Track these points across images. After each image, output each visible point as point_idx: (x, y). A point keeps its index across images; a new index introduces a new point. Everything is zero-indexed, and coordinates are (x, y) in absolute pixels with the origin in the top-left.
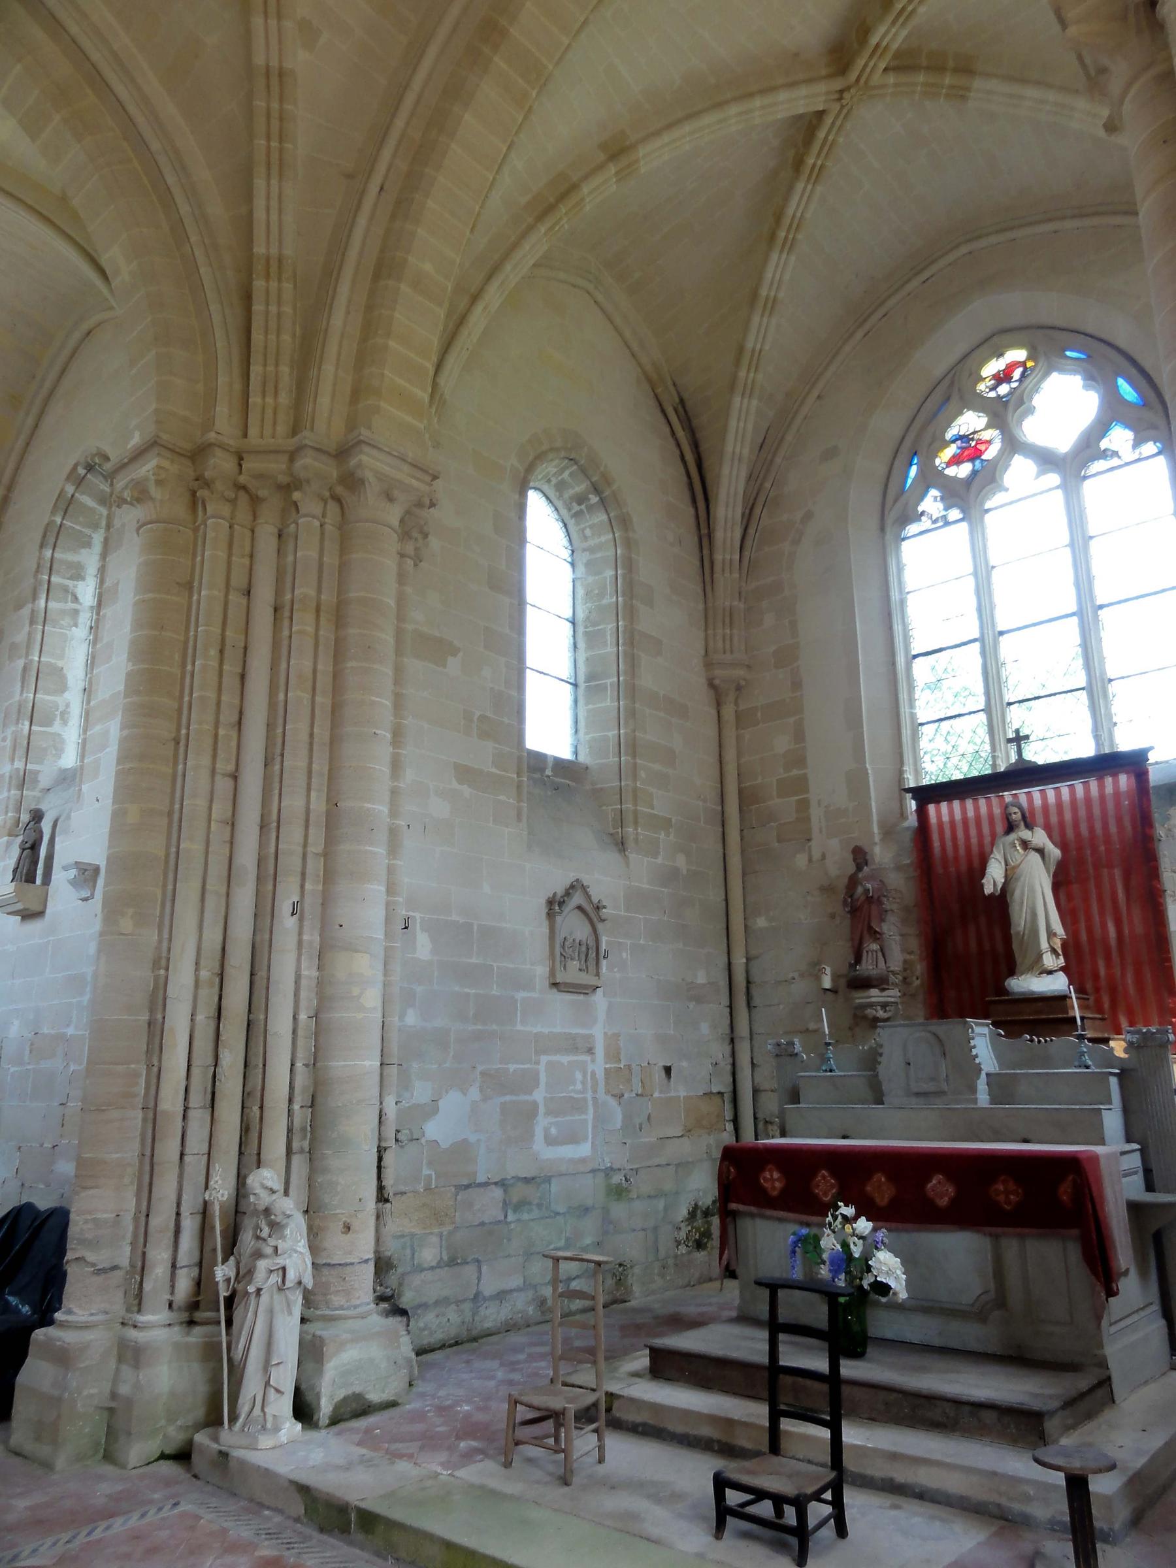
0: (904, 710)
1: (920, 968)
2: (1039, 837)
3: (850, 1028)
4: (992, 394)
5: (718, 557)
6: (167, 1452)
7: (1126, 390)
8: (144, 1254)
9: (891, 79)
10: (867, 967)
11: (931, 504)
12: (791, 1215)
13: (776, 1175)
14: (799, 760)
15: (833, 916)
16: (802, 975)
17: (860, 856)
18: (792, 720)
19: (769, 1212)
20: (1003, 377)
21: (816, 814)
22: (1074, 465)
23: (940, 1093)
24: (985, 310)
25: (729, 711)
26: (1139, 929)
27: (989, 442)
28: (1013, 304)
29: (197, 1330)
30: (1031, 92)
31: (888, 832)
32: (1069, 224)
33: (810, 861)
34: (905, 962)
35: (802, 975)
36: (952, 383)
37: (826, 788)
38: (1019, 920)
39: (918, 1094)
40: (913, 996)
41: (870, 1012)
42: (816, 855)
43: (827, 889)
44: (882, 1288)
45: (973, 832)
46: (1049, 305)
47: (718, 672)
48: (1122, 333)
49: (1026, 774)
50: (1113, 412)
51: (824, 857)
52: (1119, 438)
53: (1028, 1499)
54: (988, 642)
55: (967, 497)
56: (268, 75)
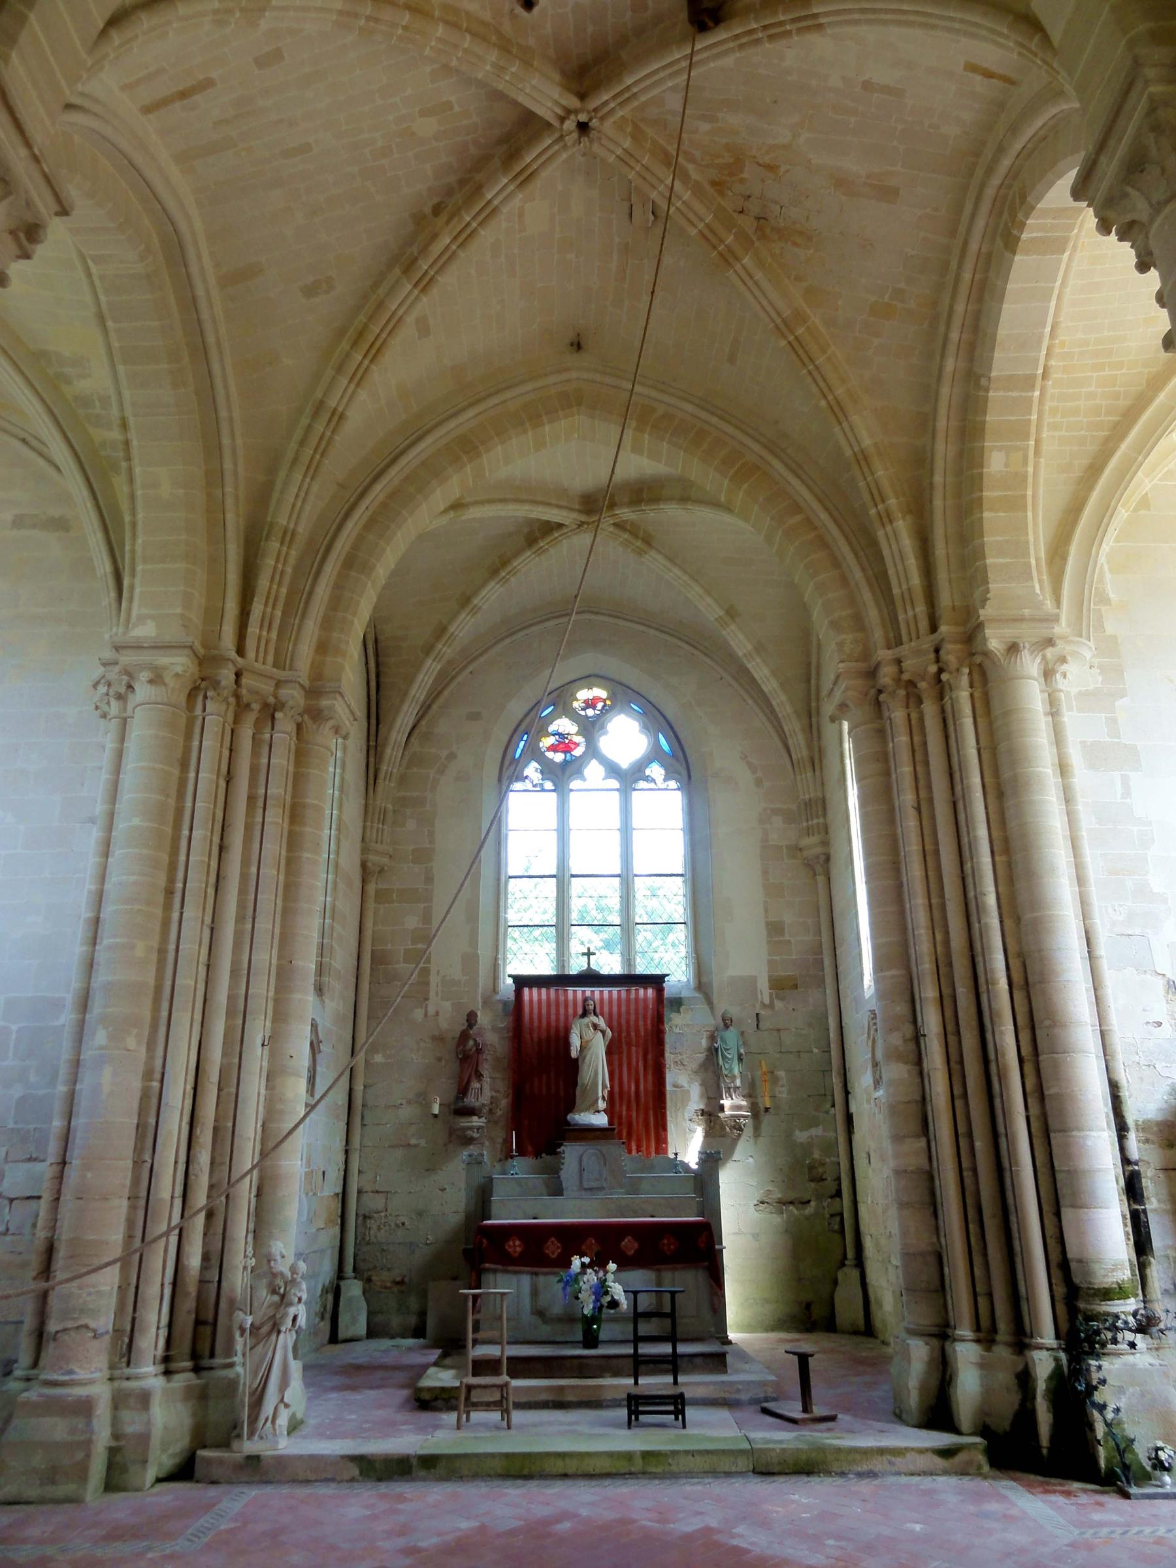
0: (502, 914)
1: (504, 1103)
2: (601, 1022)
3: (445, 1145)
4: (583, 713)
5: (384, 768)
6: (160, 1476)
7: (665, 746)
8: (134, 1319)
9: (611, 529)
10: (471, 1100)
12: (522, 1268)
13: (517, 1243)
15: (440, 1059)
16: (409, 1102)
17: (471, 1018)
18: (422, 905)
19: (510, 1268)
20: (590, 704)
21: (434, 980)
22: (629, 779)
23: (601, 1189)
25: (371, 888)
26: (650, 1087)
27: (577, 745)
28: (611, 664)
29: (177, 1377)
30: (676, 570)
31: (487, 1002)
32: (652, 632)
33: (426, 1015)
34: (492, 1097)
35: (409, 1102)
36: (559, 696)
37: (445, 960)
39: (586, 1189)
40: (496, 1123)
41: (469, 1133)
42: (431, 1010)
43: (439, 1039)
44: (614, 1304)
45: (553, 1011)
46: (631, 675)
47: (371, 857)
48: (671, 710)
49: (590, 978)
50: (656, 754)
51: (437, 1014)
52: (656, 771)
53: (738, 1391)
54: (563, 878)
56: (333, 414)
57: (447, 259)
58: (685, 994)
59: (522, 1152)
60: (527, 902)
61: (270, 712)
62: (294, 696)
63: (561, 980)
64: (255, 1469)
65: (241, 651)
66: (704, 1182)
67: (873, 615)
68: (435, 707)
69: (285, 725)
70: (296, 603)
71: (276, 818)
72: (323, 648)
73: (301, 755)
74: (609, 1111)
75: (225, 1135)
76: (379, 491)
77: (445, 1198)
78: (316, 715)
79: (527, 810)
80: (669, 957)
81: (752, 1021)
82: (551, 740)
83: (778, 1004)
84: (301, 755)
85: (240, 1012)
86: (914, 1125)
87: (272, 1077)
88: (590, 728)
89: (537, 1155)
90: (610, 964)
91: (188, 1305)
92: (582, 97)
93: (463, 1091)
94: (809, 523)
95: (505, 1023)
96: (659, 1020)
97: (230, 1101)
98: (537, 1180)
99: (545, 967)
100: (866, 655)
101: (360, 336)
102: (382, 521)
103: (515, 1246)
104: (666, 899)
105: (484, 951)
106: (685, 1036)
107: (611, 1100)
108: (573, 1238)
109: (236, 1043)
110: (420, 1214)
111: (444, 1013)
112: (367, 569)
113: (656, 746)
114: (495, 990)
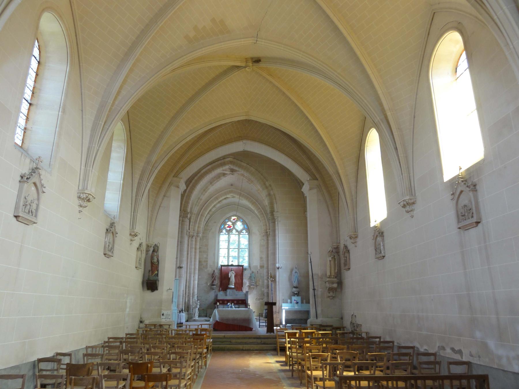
1: (219, 284)
10: (214, 283)
11: (224, 231)
14: (207, 258)
17: (214, 271)
20: (234, 220)
21: (208, 265)
22: (239, 232)
24: (234, 213)
31: (216, 268)
37: (210, 262)
38: (231, 280)
43: (209, 274)
49: (232, 265)
52: (244, 231)
60: (223, 252)
61: (193, 237)
62: (195, 234)
63: (228, 266)
64: (195, 321)
66: (246, 294)
67: (268, 225)
71: (193, 250)
72: (198, 227)
73: (196, 241)
74: (235, 285)
75: (189, 287)
77: (211, 297)
78: (198, 236)
79: (223, 237)
82: (227, 226)
84: (196, 241)
85: (190, 273)
87: (194, 281)
88: (234, 224)
90: (235, 263)
93: (213, 282)
95: (219, 272)
96: (243, 272)
100: (267, 230)
102: (206, 209)
106: (246, 274)
107: (235, 283)
108: (228, 301)
109: (190, 277)
111: (210, 270)
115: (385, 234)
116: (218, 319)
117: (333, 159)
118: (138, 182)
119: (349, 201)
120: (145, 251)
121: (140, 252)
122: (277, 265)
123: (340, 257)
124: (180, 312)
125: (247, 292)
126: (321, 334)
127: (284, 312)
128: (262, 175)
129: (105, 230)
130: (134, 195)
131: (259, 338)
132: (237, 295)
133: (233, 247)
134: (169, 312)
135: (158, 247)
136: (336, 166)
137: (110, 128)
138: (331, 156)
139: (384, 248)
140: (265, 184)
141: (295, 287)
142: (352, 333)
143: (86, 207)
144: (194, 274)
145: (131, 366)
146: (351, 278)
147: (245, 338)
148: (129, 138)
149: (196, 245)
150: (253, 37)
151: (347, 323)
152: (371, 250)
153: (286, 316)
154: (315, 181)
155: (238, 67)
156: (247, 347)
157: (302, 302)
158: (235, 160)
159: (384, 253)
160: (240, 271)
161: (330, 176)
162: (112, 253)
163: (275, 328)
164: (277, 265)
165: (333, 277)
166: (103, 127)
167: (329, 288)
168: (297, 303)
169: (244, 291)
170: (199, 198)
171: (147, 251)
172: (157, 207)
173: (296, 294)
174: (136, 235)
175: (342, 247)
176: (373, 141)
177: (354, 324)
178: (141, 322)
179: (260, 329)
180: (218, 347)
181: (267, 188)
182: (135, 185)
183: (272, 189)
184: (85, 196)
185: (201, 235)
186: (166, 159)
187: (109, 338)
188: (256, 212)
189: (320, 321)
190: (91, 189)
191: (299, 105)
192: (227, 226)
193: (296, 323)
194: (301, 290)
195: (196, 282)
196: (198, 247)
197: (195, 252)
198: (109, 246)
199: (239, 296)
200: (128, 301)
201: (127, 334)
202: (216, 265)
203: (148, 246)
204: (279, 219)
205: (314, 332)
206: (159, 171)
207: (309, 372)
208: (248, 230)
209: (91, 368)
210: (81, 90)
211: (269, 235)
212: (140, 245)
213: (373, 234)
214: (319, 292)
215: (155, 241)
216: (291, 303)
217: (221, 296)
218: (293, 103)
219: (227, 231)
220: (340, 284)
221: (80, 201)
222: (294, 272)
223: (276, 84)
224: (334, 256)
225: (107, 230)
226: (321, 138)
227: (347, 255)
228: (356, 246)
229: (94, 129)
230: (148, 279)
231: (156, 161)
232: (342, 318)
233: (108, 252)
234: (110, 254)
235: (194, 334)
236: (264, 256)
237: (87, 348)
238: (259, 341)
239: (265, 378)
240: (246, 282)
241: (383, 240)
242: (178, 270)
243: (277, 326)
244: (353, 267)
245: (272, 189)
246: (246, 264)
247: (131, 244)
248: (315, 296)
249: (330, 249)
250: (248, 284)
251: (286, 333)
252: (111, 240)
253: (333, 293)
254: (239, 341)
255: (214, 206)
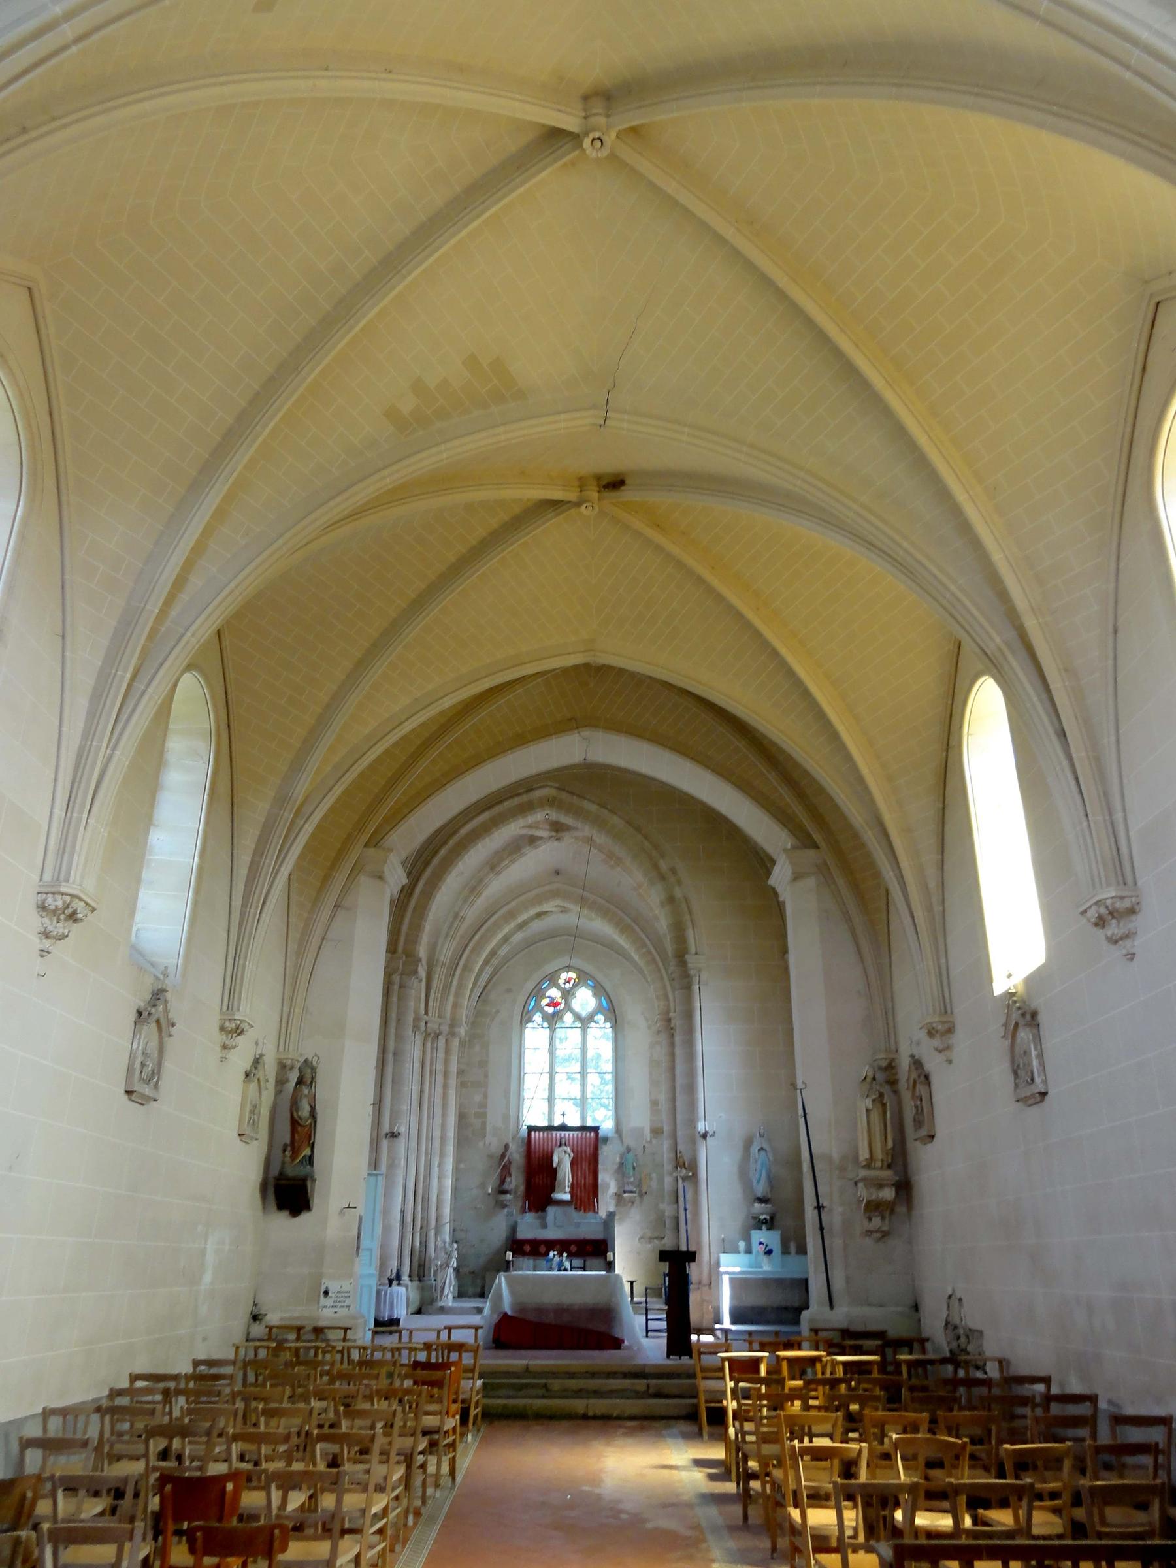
1: (522, 1189)
2: (569, 1150)
11: (537, 1017)
14: (483, 1105)
17: (506, 1147)
21: (489, 1128)
22: (585, 1022)
28: (577, 962)
37: (494, 1119)
38: (560, 1175)
43: (491, 1156)
49: (563, 1127)
52: (600, 1018)
55: (553, 1020)
57: (507, 866)
58: (610, 1135)
59: (530, 1210)
62: (445, 1029)
63: (550, 1128)
65: (426, 1013)
68: (489, 987)
69: (442, 1040)
70: (446, 990)
71: (439, 1078)
72: (455, 1005)
73: (447, 1051)
74: (572, 1193)
75: (426, 1200)
76: (477, 937)
77: (496, 1230)
78: (452, 1034)
79: (535, 1036)
80: (604, 1119)
81: (640, 1149)
82: (547, 1001)
83: (654, 1141)
84: (447, 1051)
85: (429, 1155)
86: (673, 1198)
88: (567, 994)
89: (537, 1211)
90: (574, 1121)
91: (416, 1259)
92: (557, 831)
93: (503, 1182)
94: (650, 952)
95: (523, 1149)
96: (596, 1148)
97: (427, 1188)
98: (537, 1222)
99: (544, 1123)
101: (474, 888)
103: (527, 1248)
104: (601, 1087)
105: (512, 1113)
106: (609, 1157)
108: (551, 1245)
109: (428, 1166)
110: (482, 1241)
111: (493, 1144)
112: (471, 970)
113: (600, 1004)
114: (518, 1131)
115: (1042, 1018)
116: (507, 1307)
117: (861, 779)
118: (252, 862)
119: (919, 914)
120: (272, 1081)
121: (253, 1086)
122: (701, 1127)
123: (898, 1098)
124: (391, 1282)
125: (611, 1215)
126: (845, 1364)
127: (726, 1280)
128: (646, 837)
129: (134, 1015)
130: (237, 903)
131: (640, 1373)
132: (578, 1225)
133: (567, 1070)
134: (346, 1286)
135: (313, 1069)
136: (872, 801)
137: (150, 690)
138: (855, 769)
139: (1042, 1064)
140: (656, 866)
141: (761, 1200)
142: (953, 1360)
143: (63, 937)
144: (442, 1155)
145: (168, 1487)
146: (939, 1167)
147: (593, 1375)
148: (224, 726)
149: (447, 1061)
150: (594, 407)
151: (933, 1326)
152: (1000, 1073)
153: (734, 1297)
154: (811, 853)
155: (555, 505)
156: (599, 1406)
157: (785, 1251)
158: (564, 796)
159: (1045, 1082)
160: (588, 1150)
161: (856, 836)
162: (156, 1086)
163: (694, 1337)
164: (701, 1127)
165: (879, 1164)
166: (129, 686)
167: (868, 1203)
168: (769, 1252)
169: (603, 1213)
170: (456, 916)
171: (280, 1082)
172: (315, 941)
173: (765, 1222)
174: (239, 1031)
175: (904, 1063)
176: (987, 712)
177: (956, 1327)
178: (255, 1318)
179: (645, 1341)
180: (505, 1406)
181: (662, 878)
182: (242, 872)
183: (679, 883)
184: (60, 904)
185: (462, 1031)
186: (338, 791)
187: (134, 1378)
188: (636, 957)
189: (842, 1315)
190: (83, 881)
191: (750, 615)
192: (545, 1001)
193: (767, 1323)
194: (778, 1212)
195: (448, 1183)
196: (453, 1068)
197: (445, 1087)
198: (143, 1065)
199: (585, 1227)
200: (210, 1247)
201: (196, 1363)
202: (512, 1126)
203: (283, 1067)
204: (704, 976)
205: (819, 1359)
206: (319, 827)
207: (795, 1514)
208: (613, 1013)
209: (29, 1494)
210: (63, 574)
211: (676, 1031)
212: (257, 1062)
213: (1003, 1020)
214: (835, 1217)
215: (305, 1049)
216: (749, 1251)
217: (529, 1228)
218: (730, 607)
219: (546, 1017)
220: (905, 1187)
221: (46, 920)
222: (754, 1149)
223: (675, 550)
224: (881, 1095)
225: (140, 1013)
226: (821, 715)
227: (921, 1089)
228: (950, 1062)
229: (98, 696)
230: (281, 1173)
231: (307, 798)
232: (916, 1308)
233: (142, 1084)
234: (147, 1091)
235: (416, 1365)
236: (663, 1097)
237: (47, 1413)
238: (640, 1385)
239: (650, 1525)
240: (608, 1182)
241: (1038, 1039)
242: (385, 1143)
243: (699, 1332)
244: (941, 1130)
245: (679, 883)
246: (607, 1125)
247: (223, 1059)
248: (822, 1229)
249: (866, 1070)
250: (613, 1188)
251: (723, 1359)
252: (154, 1044)
253: (883, 1218)
254: (573, 1384)
255: (506, 939)
